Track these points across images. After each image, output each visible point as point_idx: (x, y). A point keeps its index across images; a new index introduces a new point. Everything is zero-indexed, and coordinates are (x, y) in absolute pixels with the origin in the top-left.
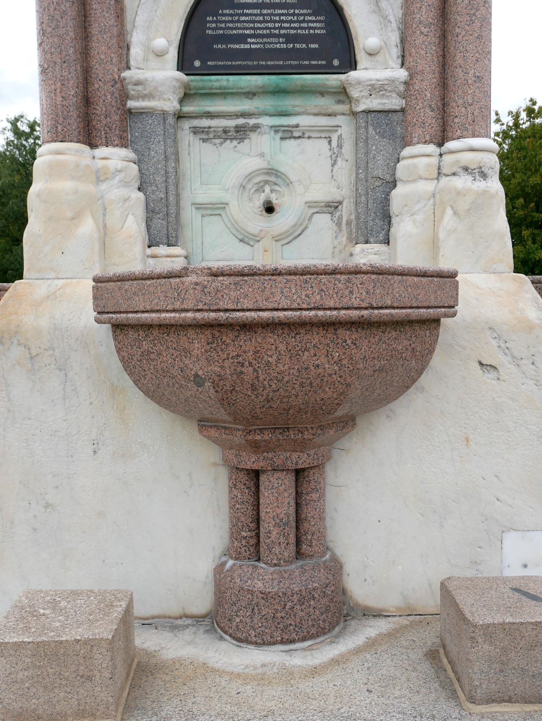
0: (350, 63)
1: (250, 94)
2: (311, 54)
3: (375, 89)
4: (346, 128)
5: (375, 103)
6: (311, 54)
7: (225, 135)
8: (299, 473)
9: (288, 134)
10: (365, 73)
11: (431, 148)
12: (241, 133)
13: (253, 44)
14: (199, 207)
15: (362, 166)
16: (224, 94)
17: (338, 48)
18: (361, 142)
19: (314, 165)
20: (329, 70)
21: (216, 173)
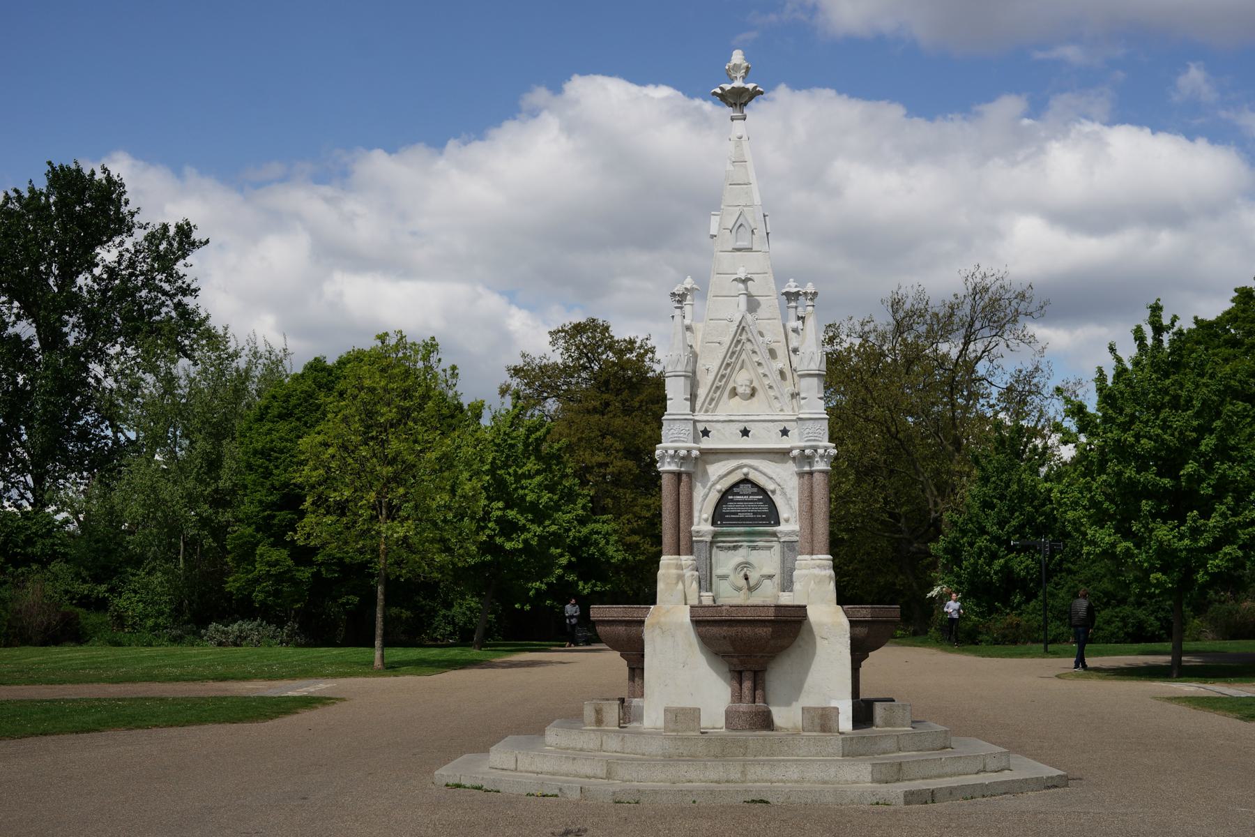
0: (778, 523)
1: (739, 534)
2: (763, 519)
3: (787, 534)
4: (777, 546)
5: (787, 539)
6: (763, 519)
7: (729, 548)
8: (756, 673)
9: (754, 548)
10: (783, 528)
11: (807, 557)
12: (735, 548)
13: (741, 516)
14: (719, 577)
15: (783, 561)
16: (729, 534)
17: (773, 516)
18: (783, 553)
19: (767, 561)
20: (769, 525)
21: (726, 562)
